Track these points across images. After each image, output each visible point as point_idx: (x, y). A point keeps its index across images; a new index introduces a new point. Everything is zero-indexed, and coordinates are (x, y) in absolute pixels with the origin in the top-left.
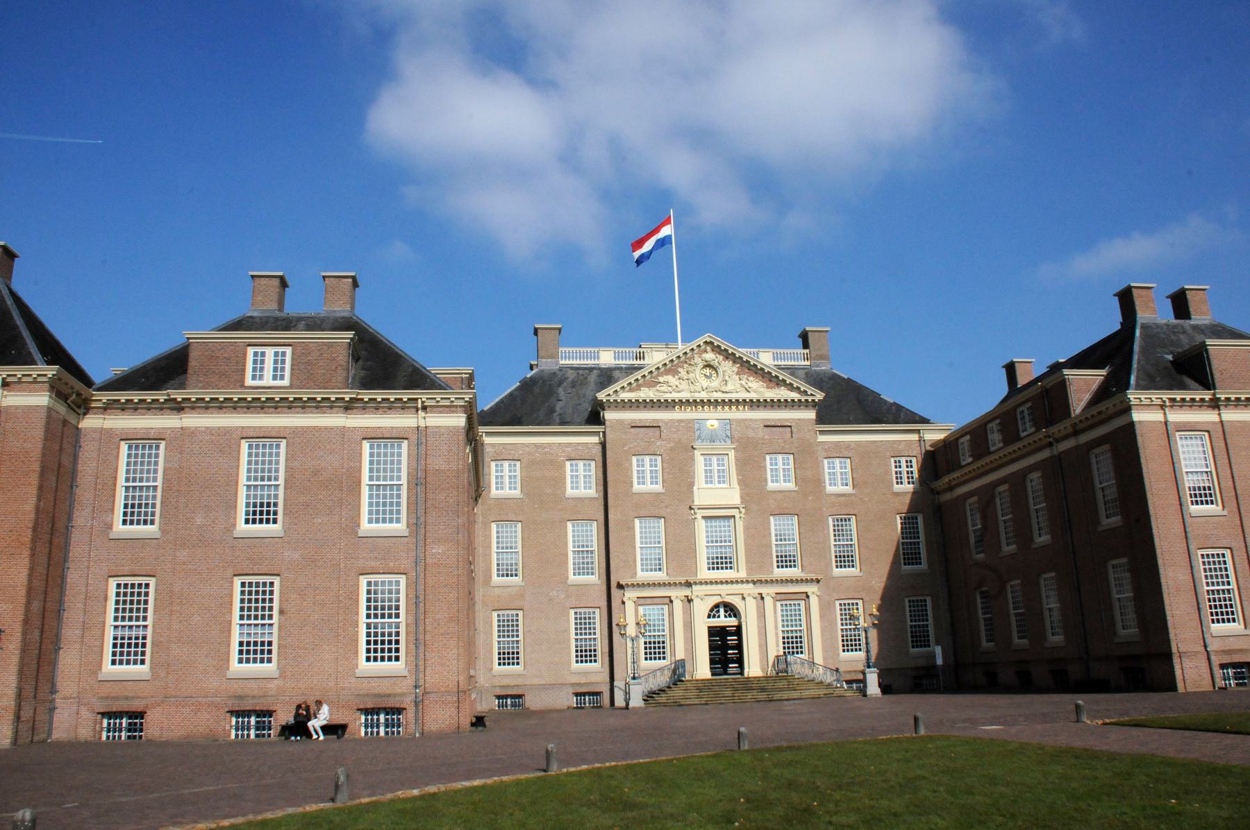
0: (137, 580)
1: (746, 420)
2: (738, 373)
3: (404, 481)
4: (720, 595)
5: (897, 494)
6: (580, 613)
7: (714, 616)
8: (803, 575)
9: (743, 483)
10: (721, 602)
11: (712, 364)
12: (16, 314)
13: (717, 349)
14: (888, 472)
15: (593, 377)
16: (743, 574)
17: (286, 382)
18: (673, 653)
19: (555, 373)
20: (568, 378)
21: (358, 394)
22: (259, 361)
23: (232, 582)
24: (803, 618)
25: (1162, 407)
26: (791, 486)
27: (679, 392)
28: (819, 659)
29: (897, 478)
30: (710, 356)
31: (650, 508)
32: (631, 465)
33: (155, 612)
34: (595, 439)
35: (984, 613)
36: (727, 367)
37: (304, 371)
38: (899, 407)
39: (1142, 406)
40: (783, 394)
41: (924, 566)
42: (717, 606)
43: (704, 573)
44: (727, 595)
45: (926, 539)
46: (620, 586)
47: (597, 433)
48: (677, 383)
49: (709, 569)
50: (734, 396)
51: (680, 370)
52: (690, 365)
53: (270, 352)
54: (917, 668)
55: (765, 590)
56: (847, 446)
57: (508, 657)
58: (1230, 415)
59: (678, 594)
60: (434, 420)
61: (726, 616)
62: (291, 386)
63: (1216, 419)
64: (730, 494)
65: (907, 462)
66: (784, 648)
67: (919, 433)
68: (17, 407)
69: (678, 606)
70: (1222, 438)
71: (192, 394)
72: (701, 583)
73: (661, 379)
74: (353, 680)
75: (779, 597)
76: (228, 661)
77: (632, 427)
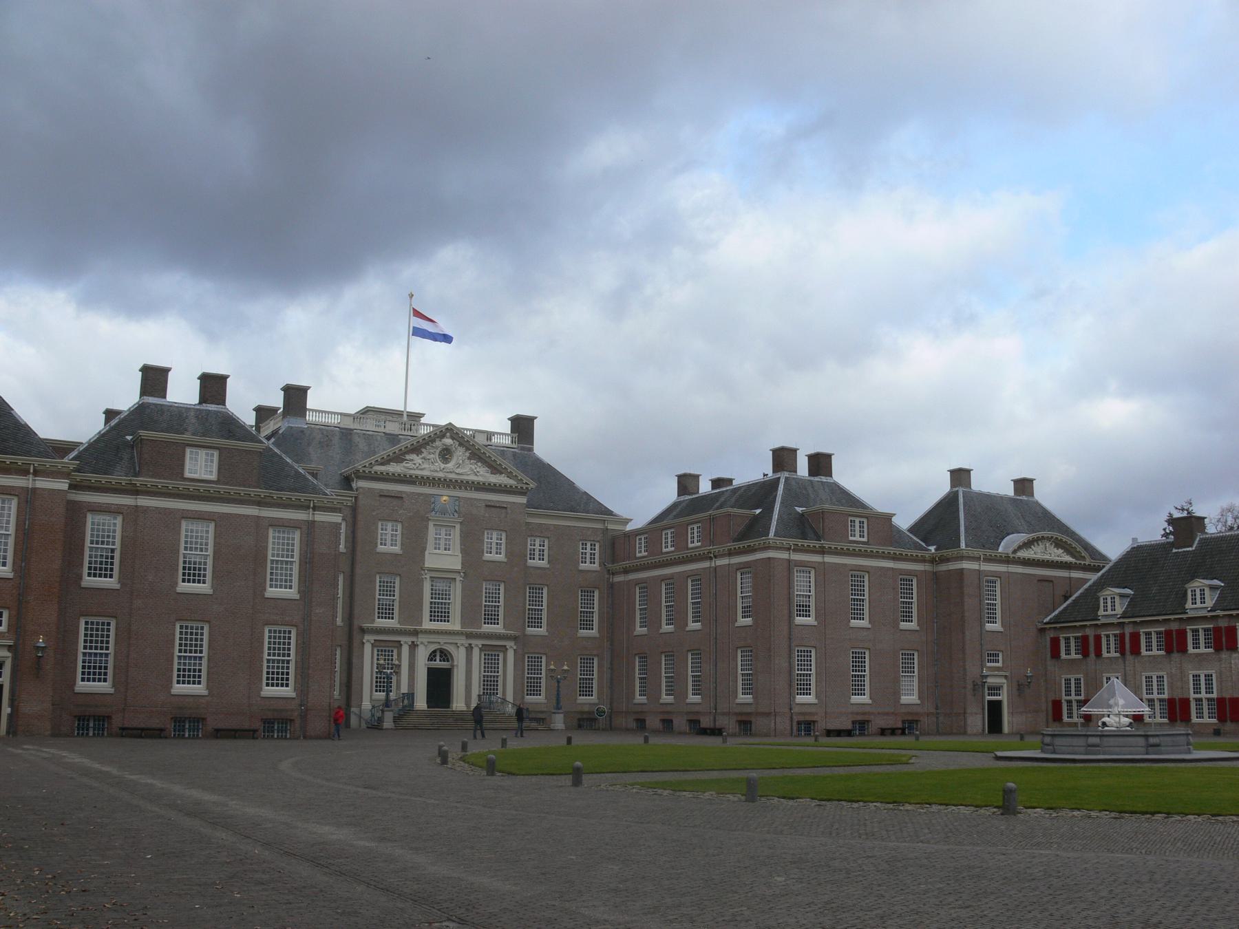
0: (101, 620)
1: (472, 499)
2: (469, 458)
3: (296, 558)
4: (439, 643)
6: (187, 627)
7: (431, 660)
9: (462, 551)
10: (438, 649)
11: (450, 448)
15: (336, 440)
16: (457, 627)
17: (213, 477)
18: (398, 687)
19: (302, 432)
20: (314, 438)
21: (271, 493)
23: (175, 625)
24: (501, 666)
25: (789, 549)
26: (501, 557)
27: (421, 469)
28: (510, 698)
29: (582, 558)
30: (448, 441)
31: (391, 564)
32: (377, 528)
33: (116, 644)
35: (640, 674)
36: (460, 454)
41: (594, 632)
42: (434, 652)
44: (445, 643)
45: (599, 610)
46: (363, 631)
48: (420, 461)
49: (431, 620)
51: (423, 450)
52: (433, 447)
53: (202, 454)
54: (582, 713)
55: (474, 642)
58: (829, 559)
59: (406, 640)
60: (320, 517)
61: (440, 661)
63: (822, 561)
64: (452, 560)
65: (591, 545)
66: (484, 689)
67: (604, 524)
68: (44, 489)
69: (405, 650)
70: (823, 572)
73: (408, 457)
74: (259, 699)
76: (171, 682)
77: (381, 496)
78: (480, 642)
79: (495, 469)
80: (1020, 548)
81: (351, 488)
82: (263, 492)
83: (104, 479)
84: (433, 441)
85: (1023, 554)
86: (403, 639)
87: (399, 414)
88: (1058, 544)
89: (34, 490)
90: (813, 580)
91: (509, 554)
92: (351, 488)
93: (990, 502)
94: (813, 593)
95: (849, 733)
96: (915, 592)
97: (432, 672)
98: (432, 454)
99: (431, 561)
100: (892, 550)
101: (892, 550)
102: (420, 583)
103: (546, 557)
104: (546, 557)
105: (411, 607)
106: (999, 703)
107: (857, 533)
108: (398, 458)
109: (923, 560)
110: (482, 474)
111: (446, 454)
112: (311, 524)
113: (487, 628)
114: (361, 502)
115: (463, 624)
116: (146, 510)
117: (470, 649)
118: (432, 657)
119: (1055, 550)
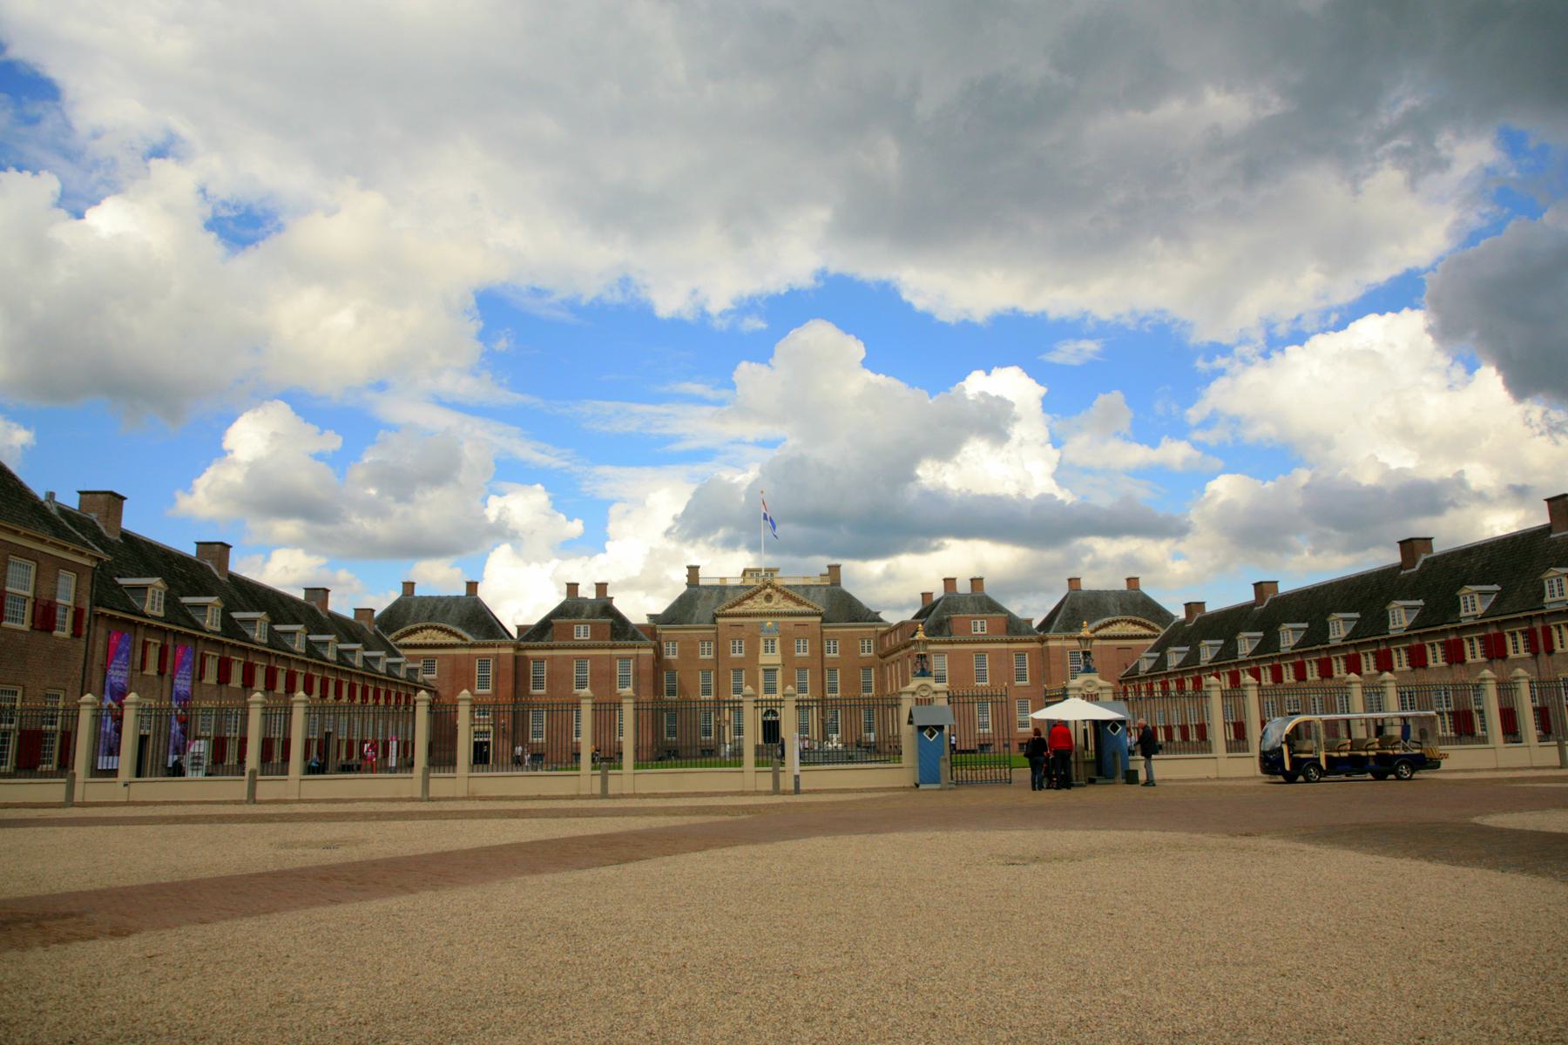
3: (631, 673)
5: (861, 658)
8: (810, 697)
9: (783, 653)
12: (495, 621)
13: (773, 587)
15: (715, 594)
17: (588, 638)
22: (579, 629)
26: (807, 654)
34: (714, 631)
36: (777, 597)
37: (595, 635)
38: (869, 611)
40: (804, 609)
47: (714, 629)
50: (780, 610)
53: (582, 627)
56: (837, 634)
57: (672, 732)
58: (956, 647)
60: (642, 652)
62: (590, 640)
71: (556, 643)
73: (745, 602)
79: (799, 603)
80: (1096, 629)
81: (715, 623)
83: (540, 643)
84: (760, 591)
87: (760, 570)
88: (1135, 623)
89: (498, 654)
90: (946, 660)
91: (811, 652)
92: (715, 623)
93: (1097, 595)
94: (946, 668)
95: (974, 752)
96: (1027, 662)
97: (764, 723)
98: (759, 599)
100: (1005, 637)
101: (1005, 637)
102: (757, 672)
103: (838, 651)
104: (838, 651)
108: (739, 603)
109: (1031, 641)
110: (791, 606)
111: (768, 598)
112: (638, 655)
114: (719, 631)
116: (556, 657)
118: (767, 714)
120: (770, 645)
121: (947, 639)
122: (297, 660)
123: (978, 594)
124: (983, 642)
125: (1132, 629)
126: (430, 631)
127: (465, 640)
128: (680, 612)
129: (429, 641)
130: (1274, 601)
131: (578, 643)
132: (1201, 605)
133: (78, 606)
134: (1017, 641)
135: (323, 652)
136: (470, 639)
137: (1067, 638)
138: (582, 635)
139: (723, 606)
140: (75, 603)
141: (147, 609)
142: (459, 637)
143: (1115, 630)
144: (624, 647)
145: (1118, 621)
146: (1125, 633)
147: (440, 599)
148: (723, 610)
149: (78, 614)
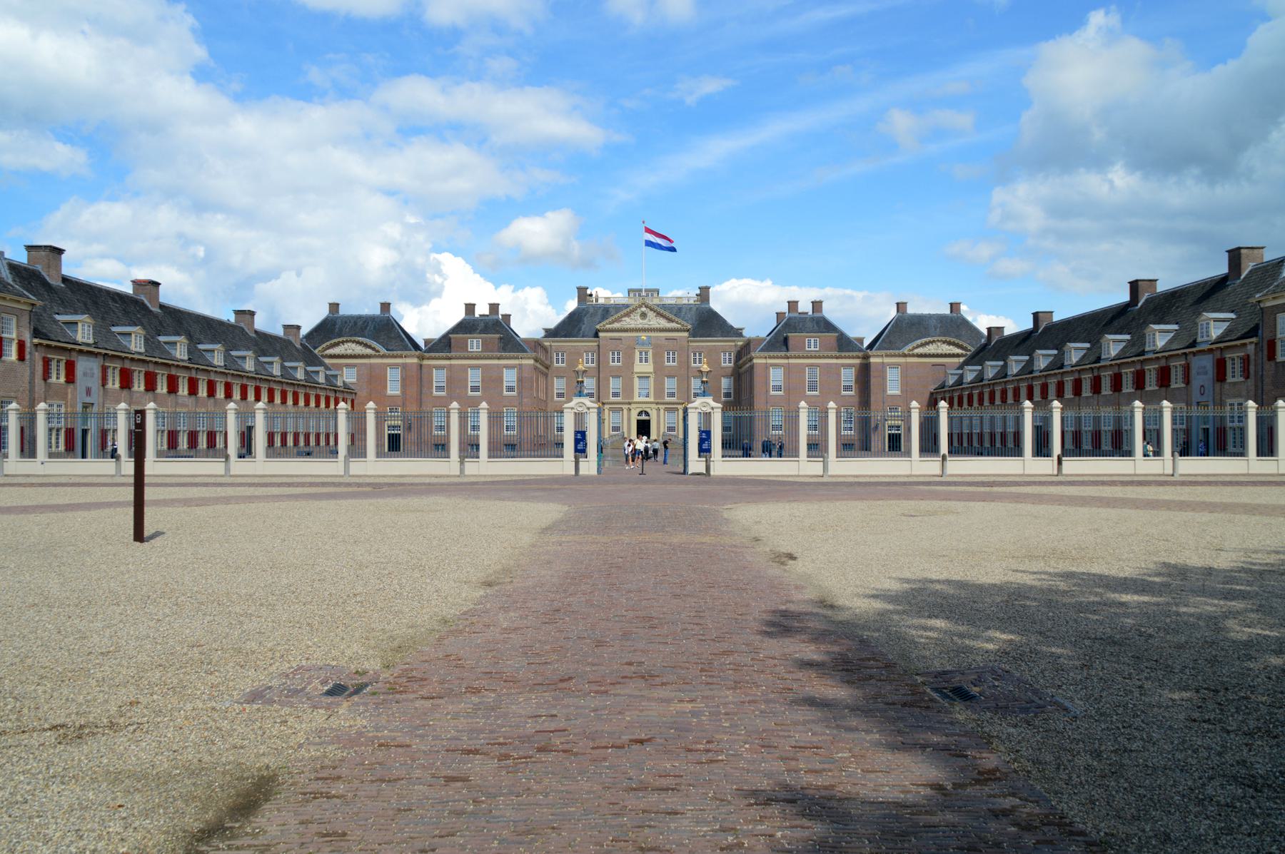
5: (724, 368)
9: (654, 363)
13: (646, 307)
14: (720, 359)
30: (644, 309)
36: (651, 314)
39: (757, 358)
40: (674, 325)
43: (637, 399)
53: (475, 340)
55: (660, 406)
56: (703, 347)
58: (791, 361)
60: (524, 362)
64: (648, 368)
69: (625, 411)
70: (788, 370)
72: (634, 403)
75: (666, 409)
78: (664, 406)
79: (670, 320)
82: (499, 354)
85: (916, 351)
86: (623, 406)
87: (640, 290)
88: (949, 343)
97: (639, 422)
99: (636, 370)
100: (834, 353)
102: (632, 380)
105: (628, 389)
106: (900, 435)
107: (812, 346)
108: (618, 320)
113: (667, 399)
115: (655, 398)
117: (658, 410)
118: (640, 414)
119: (947, 347)
120: (644, 356)
121: (783, 354)
122: (216, 372)
123: (817, 315)
124: (816, 357)
125: (946, 349)
126: (349, 344)
127: (378, 351)
128: (570, 327)
129: (349, 352)
130: (1047, 329)
131: (474, 355)
132: (1000, 329)
133: (20, 338)
134: (845, 357)
135: (243, 365)
136: (383, 351)
137: (887, 356)
138: (475, 347)
139: (604, 323)
140: (18, 336)
141: (79, 338)
142: (373, 349)
143: (931, 349)
144: (508, 358)
145: (934, 341)
146: (940, 351)
147: (360, 317)
148: (604, 325)
149: (21, 346)
